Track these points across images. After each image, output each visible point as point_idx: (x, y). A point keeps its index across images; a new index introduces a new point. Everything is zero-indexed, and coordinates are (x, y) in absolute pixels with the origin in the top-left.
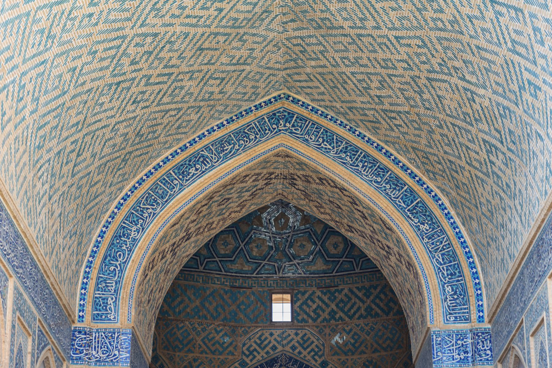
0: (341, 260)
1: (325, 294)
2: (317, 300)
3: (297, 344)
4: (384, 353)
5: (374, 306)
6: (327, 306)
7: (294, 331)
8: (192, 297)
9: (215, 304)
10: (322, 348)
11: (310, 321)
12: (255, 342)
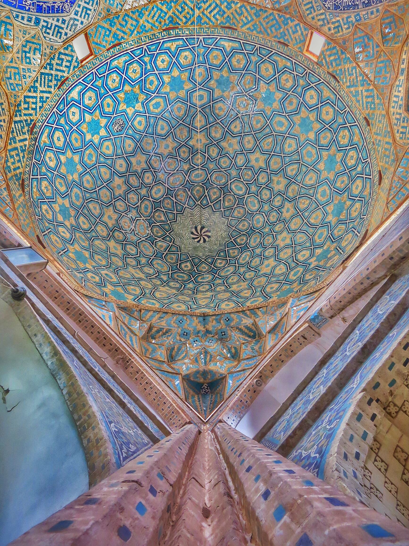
0: (66, 108)
1: (61, 77)
2: (64, 69)
3: (63, 26)
4: (6, 64)
5: (34, 95)
6: (57, 70)
7: (69, 35)
8: (146, 24)
9: (129, 26)
10: (45, 35)
11: (62, 51)
12: (90, 10)
